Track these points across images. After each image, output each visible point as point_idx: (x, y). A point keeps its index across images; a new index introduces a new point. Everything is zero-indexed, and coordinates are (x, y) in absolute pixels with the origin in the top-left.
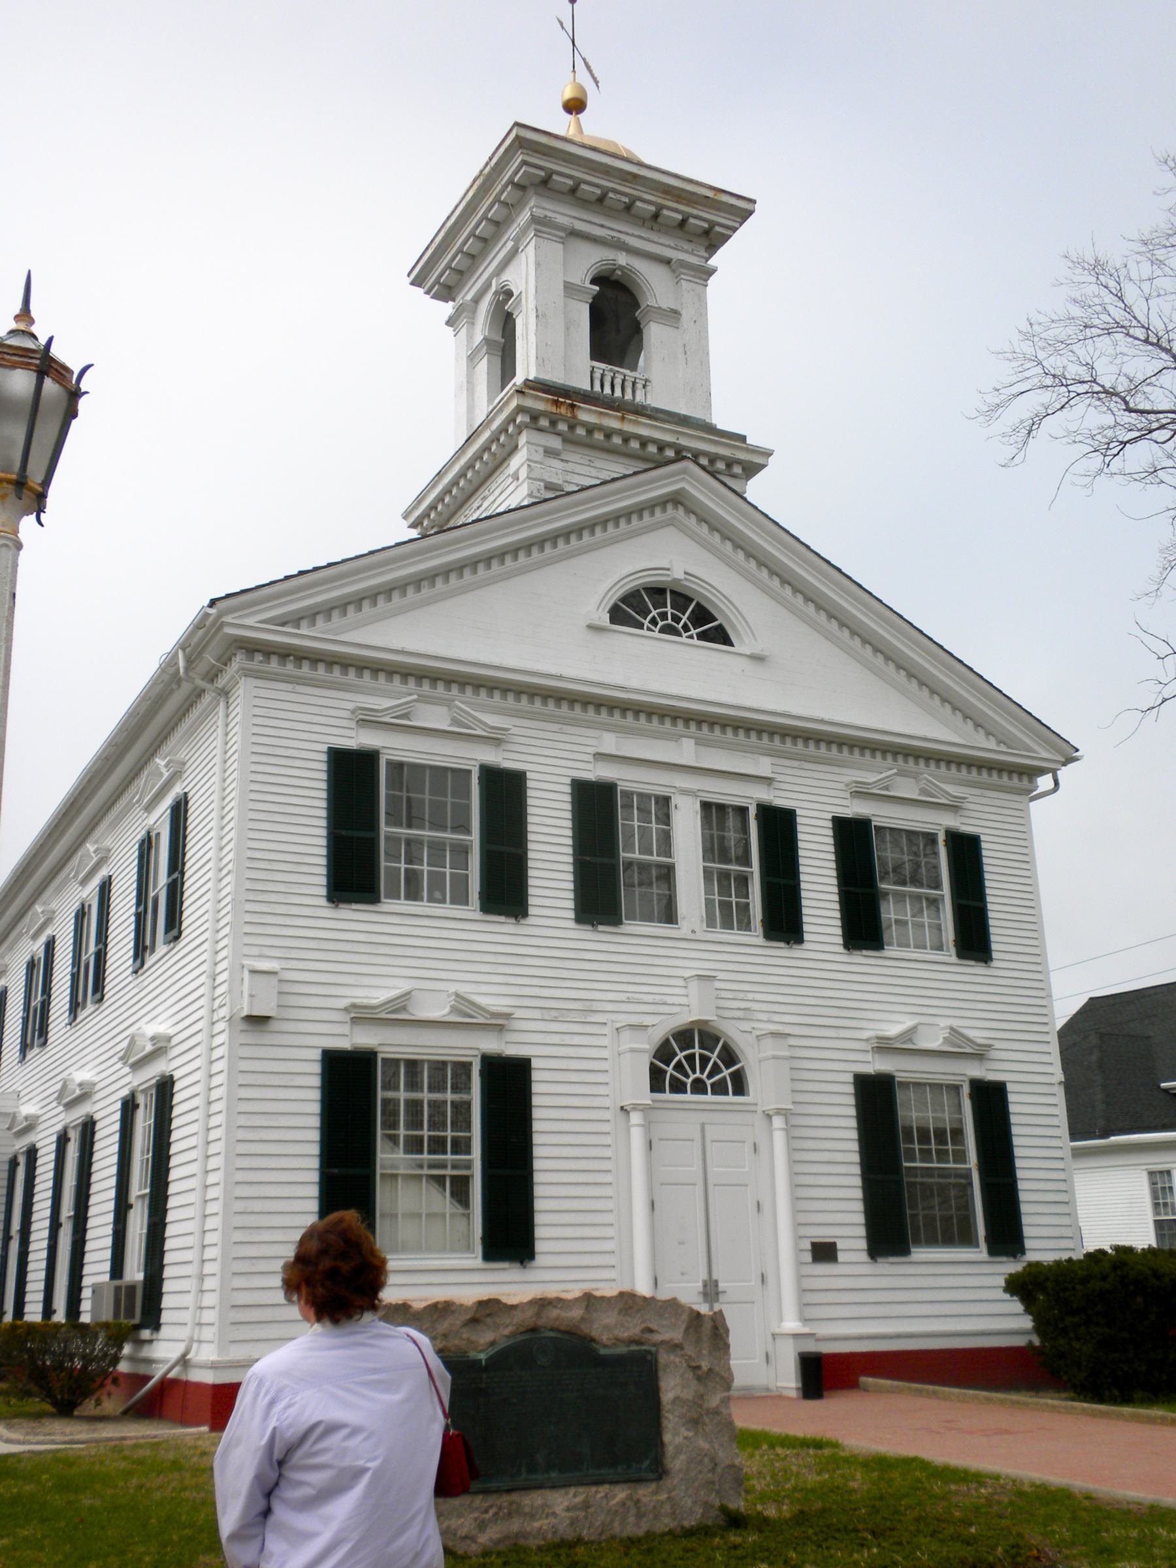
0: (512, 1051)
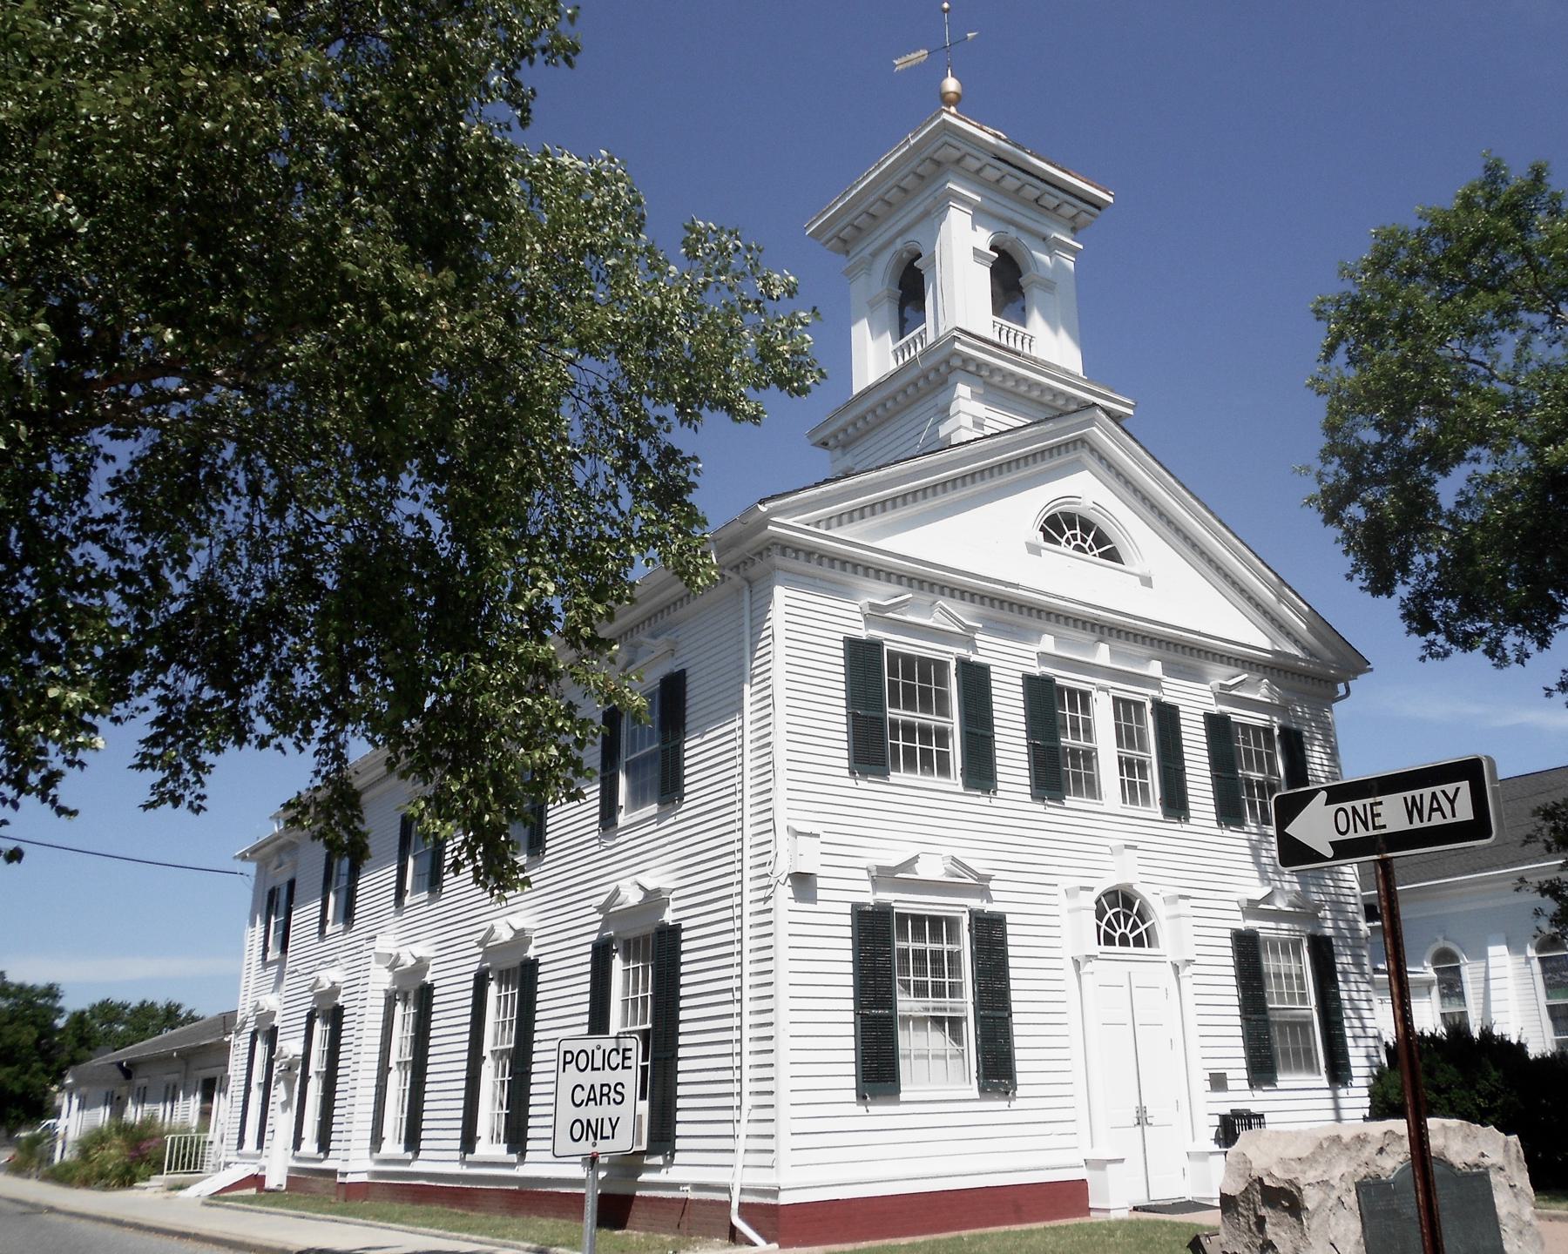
0: (989, 908)
